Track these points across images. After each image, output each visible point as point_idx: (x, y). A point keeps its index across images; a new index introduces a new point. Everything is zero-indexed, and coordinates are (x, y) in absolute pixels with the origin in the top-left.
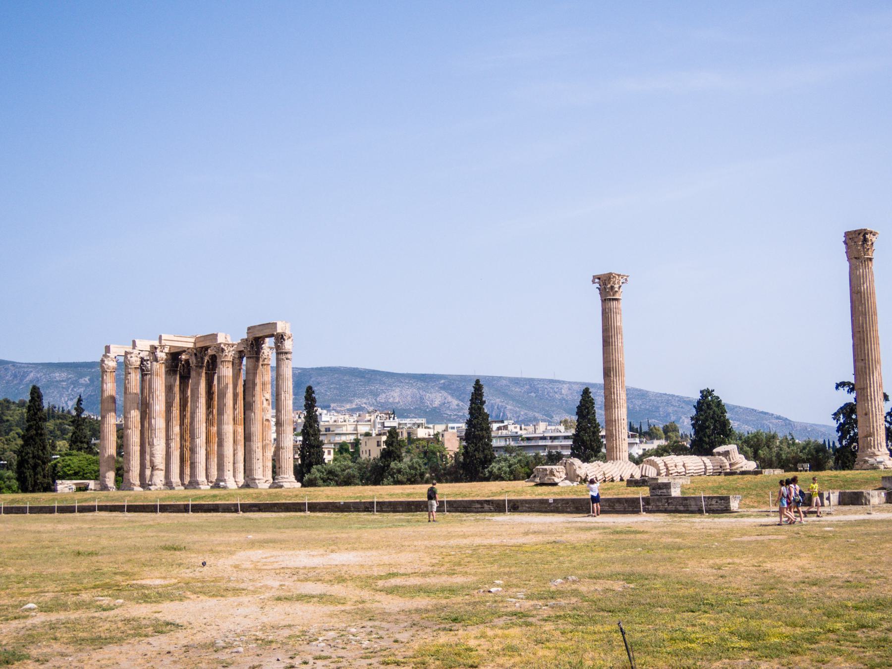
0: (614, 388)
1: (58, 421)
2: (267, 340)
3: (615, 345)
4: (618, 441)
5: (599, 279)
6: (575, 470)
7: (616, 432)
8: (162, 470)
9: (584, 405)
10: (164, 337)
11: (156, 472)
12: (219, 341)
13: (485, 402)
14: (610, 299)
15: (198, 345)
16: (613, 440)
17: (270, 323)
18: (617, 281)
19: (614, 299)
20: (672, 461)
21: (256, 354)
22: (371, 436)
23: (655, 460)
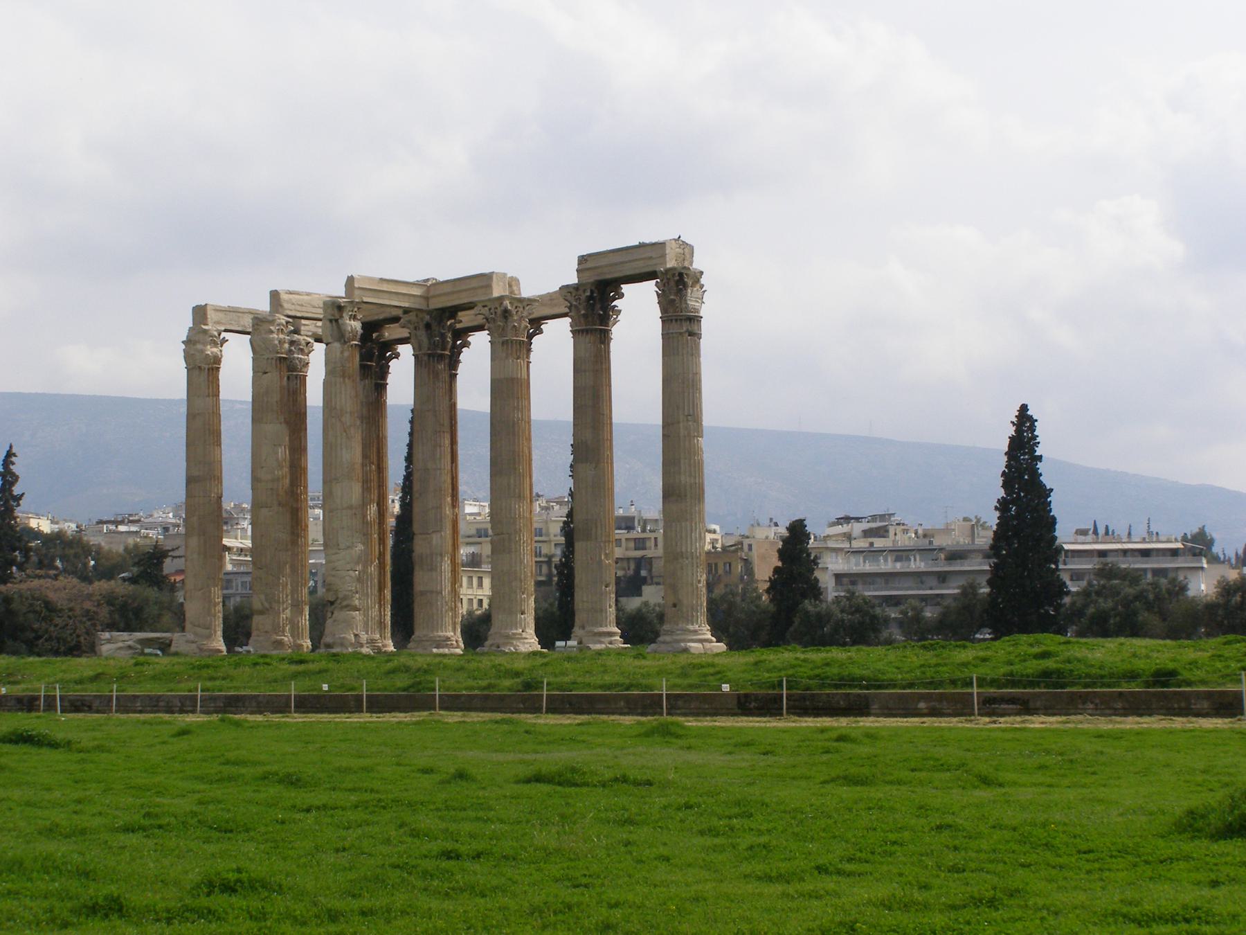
2: (626, 288)
8: (358, 610)
12: (496, 294)
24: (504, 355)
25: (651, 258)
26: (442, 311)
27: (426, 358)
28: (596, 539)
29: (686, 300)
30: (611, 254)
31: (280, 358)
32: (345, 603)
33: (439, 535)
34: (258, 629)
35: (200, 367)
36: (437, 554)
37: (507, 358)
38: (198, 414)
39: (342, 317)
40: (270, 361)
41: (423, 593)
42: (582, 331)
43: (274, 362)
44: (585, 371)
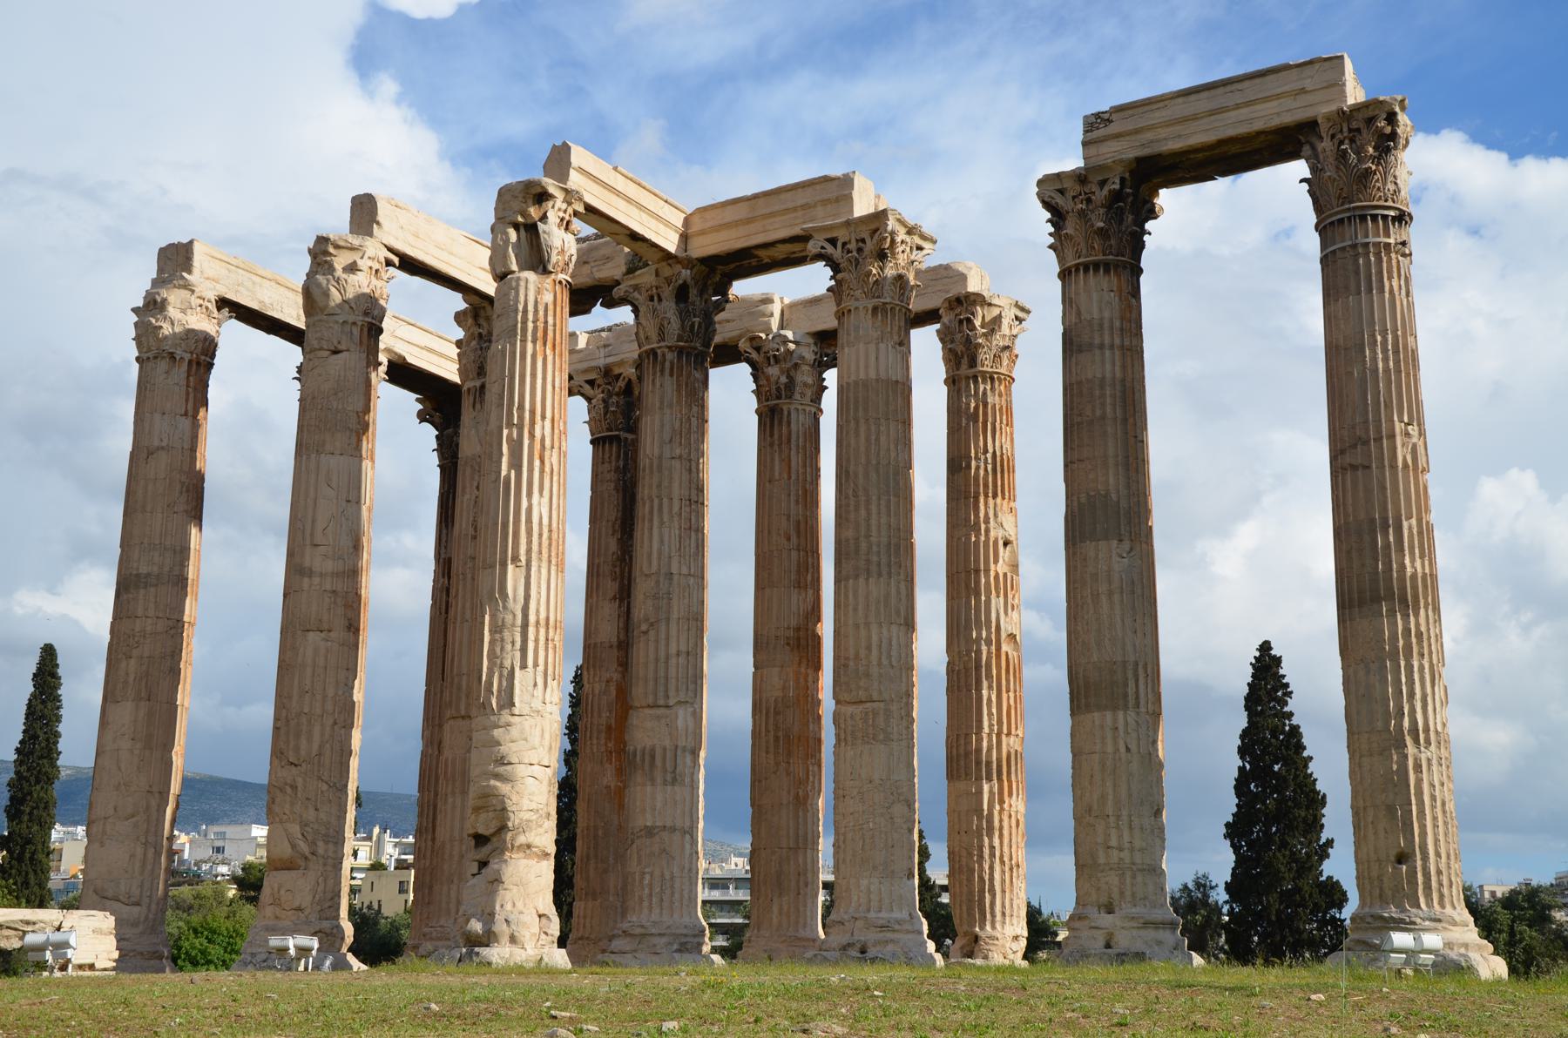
15: (705, 247)
17: (1286, 67)
25: (1303, 91)
26: (710, 262)
28: (1137, 705)
29: (1395, 177)
30: (1180, 100)
32: (522, 839)
34: (276, 902)
36: (684, 749)
38: (163, 448)
39: (544, 218)
40: (348, 328)
41: (650, 832)
42: (1096, 266)
43: (356, 331)
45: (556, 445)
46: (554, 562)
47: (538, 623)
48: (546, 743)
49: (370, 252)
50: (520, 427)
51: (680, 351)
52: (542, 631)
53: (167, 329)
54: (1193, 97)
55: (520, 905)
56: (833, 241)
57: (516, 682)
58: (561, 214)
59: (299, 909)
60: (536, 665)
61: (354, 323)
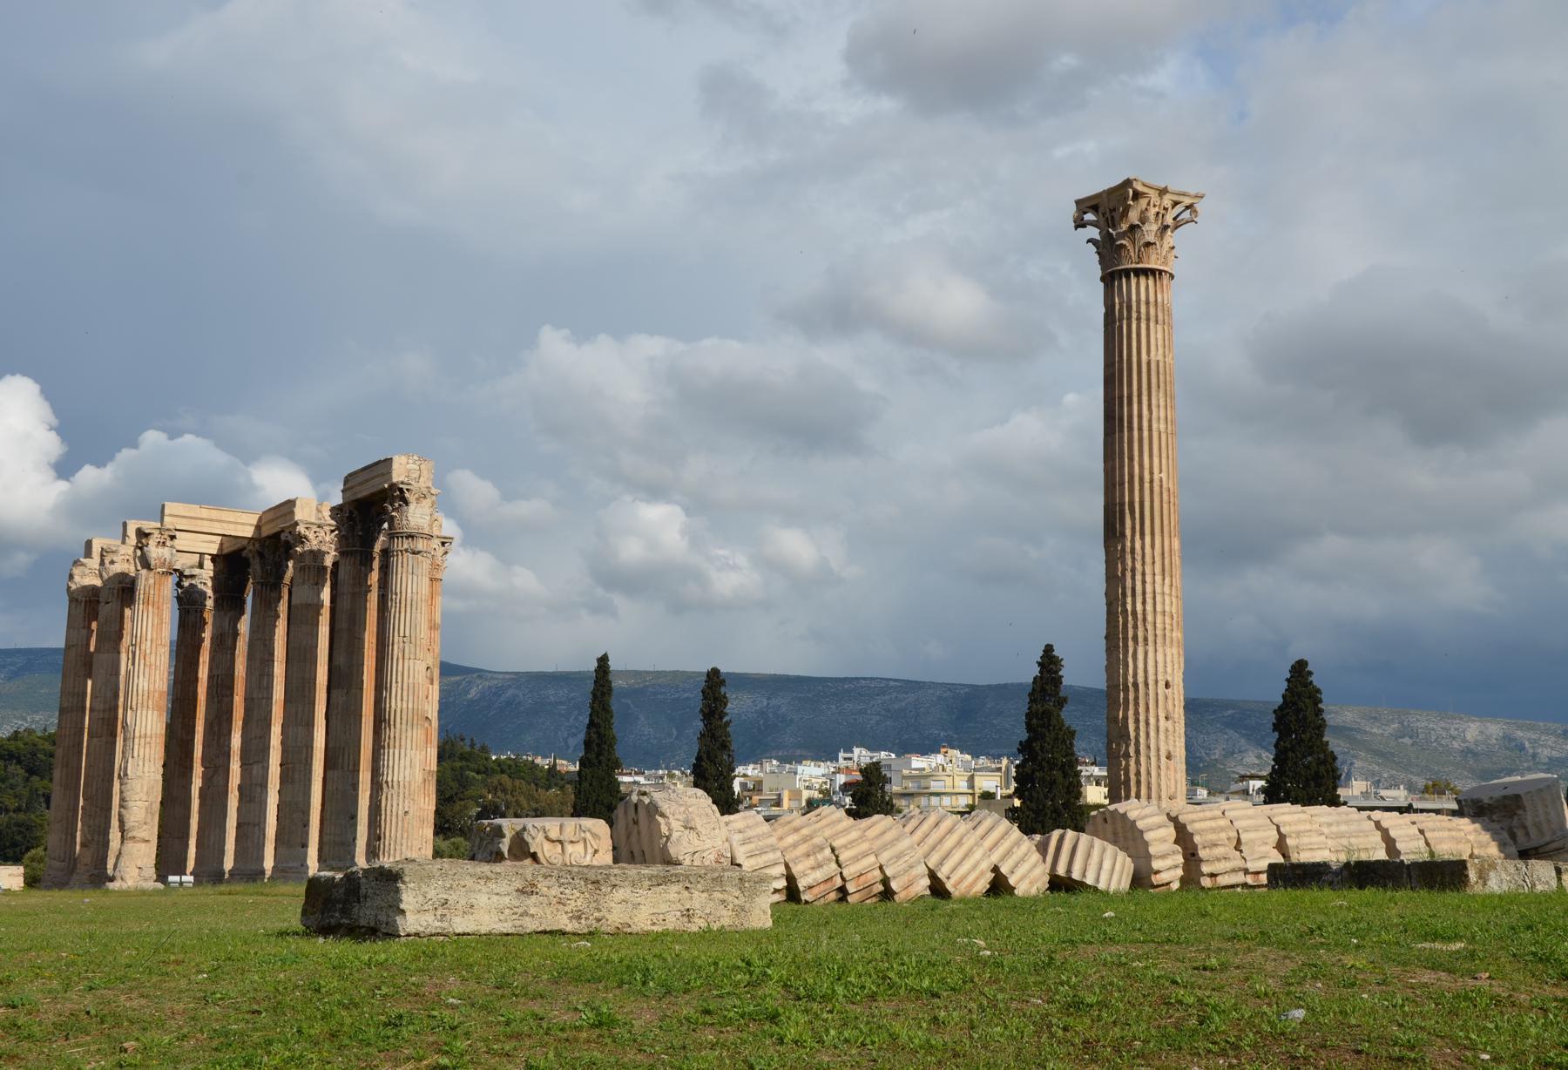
0: (1133, 578)
1: (458, 764)
3: (1140, 429)
4: (1143, 759)
5: (1095, 209)
6: (668, 838)
7: (1137, 729)
8: (147, 841)
9: (1295, 704)
10: (170, 508)
11: (129, 846)
13: (1065, 700)
14: (1127, 273)
15: (266, 532)
16: (1127, 756)
18: (1153, 211)
19: (1139, 272)
20: (1223, 823)
21: (362, 546)
22: (994, 798)
23: (1121, 811)
24: (301, 580)
27: (259, 587)
28: (342, 768)
31: (123, 589)
32: (130, 835)
33: (261, 765)
35: (77, 600)
36: (256, 785)
37: (303, 583)
38: (73, 646)
43: (115, 592)
44: (344, 594)
45: (153, 652)
46: (151, 706)
47: (140, 736)
48: (145, 789)
49: (122, 552)
50: (135, 645)
51: (262, 584)
52: (143, 740)
53: (74, 587)
54: (365, 472)
55: (127, 864)
56: (290, 533)
57: (129, 765)
58: (157, 540)
59: (86, 865)
60: (138, 756)
61: (114, 588)
